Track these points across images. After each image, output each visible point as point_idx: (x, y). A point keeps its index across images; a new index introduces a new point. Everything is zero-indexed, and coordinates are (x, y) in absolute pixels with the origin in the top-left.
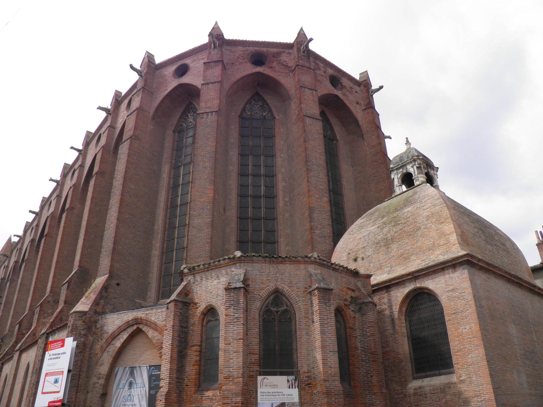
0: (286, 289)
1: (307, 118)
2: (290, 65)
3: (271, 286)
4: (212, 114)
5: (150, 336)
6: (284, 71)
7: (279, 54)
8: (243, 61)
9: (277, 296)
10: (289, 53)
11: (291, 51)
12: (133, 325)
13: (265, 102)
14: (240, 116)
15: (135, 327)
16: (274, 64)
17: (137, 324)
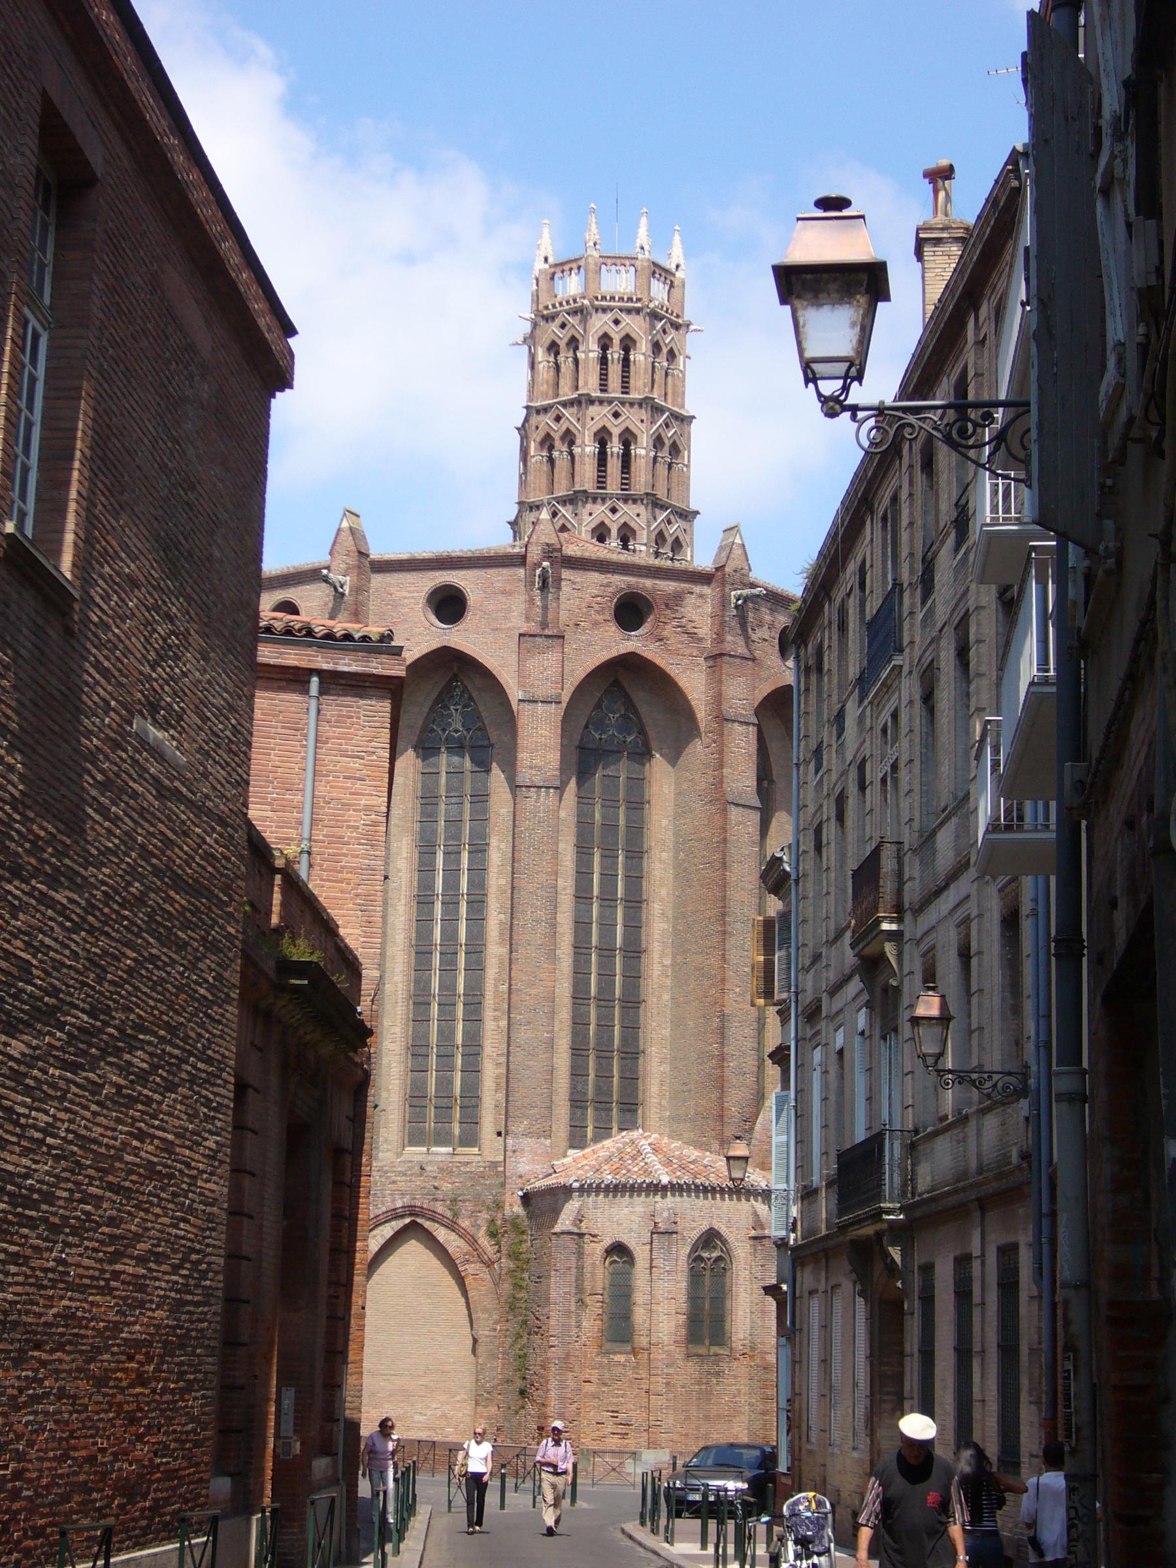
0: (723, 1230)
1: (733, 808)
2: (701, 633)
3: (705, 1227)
4: (547, 793)
5: (441, 1239)
6: (688, 652)
7: (677, 599)
8: (600, 618)
9: (711, 1238)
10: (701, 596)
11: (706, 590)
12: (403, 1216)
13: (630, 705)
14: (581, 748)
15: (407, 1220)
16: (668, 631)
17: (411, 1215)
